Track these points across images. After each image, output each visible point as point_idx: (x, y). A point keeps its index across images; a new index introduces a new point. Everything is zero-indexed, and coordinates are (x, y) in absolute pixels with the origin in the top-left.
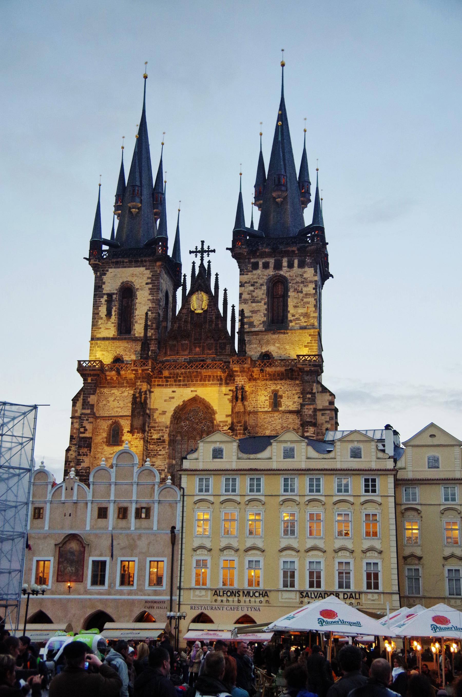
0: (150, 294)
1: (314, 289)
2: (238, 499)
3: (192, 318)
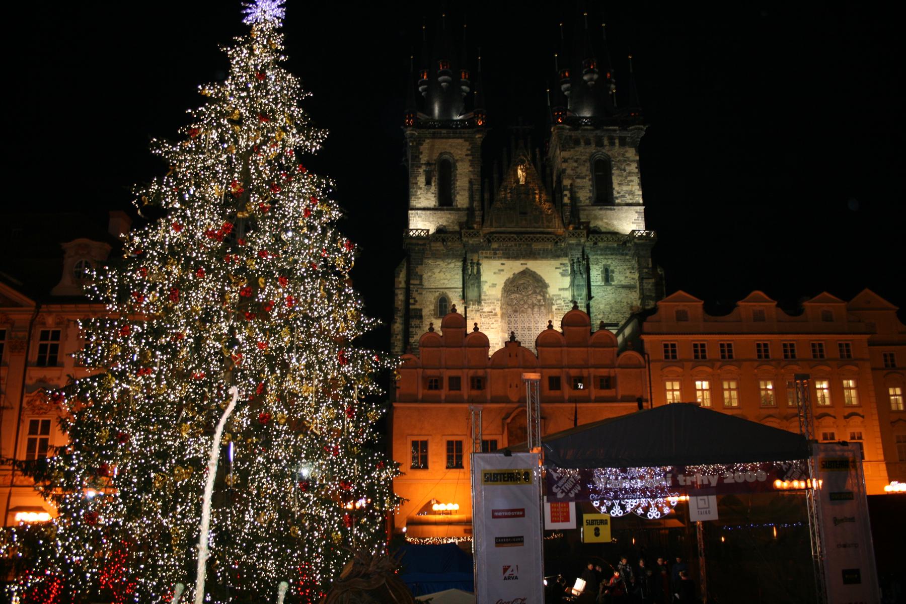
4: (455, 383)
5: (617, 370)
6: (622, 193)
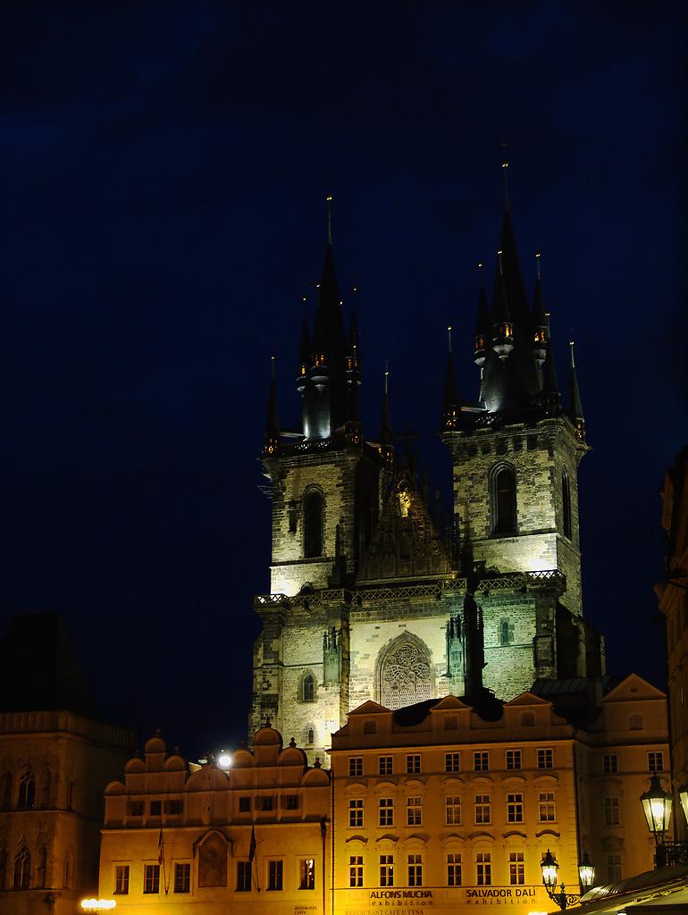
0: (342, 500)
1: (549, 478)
4: (156, 808)
5: (302, 789)
6: (529, 517)
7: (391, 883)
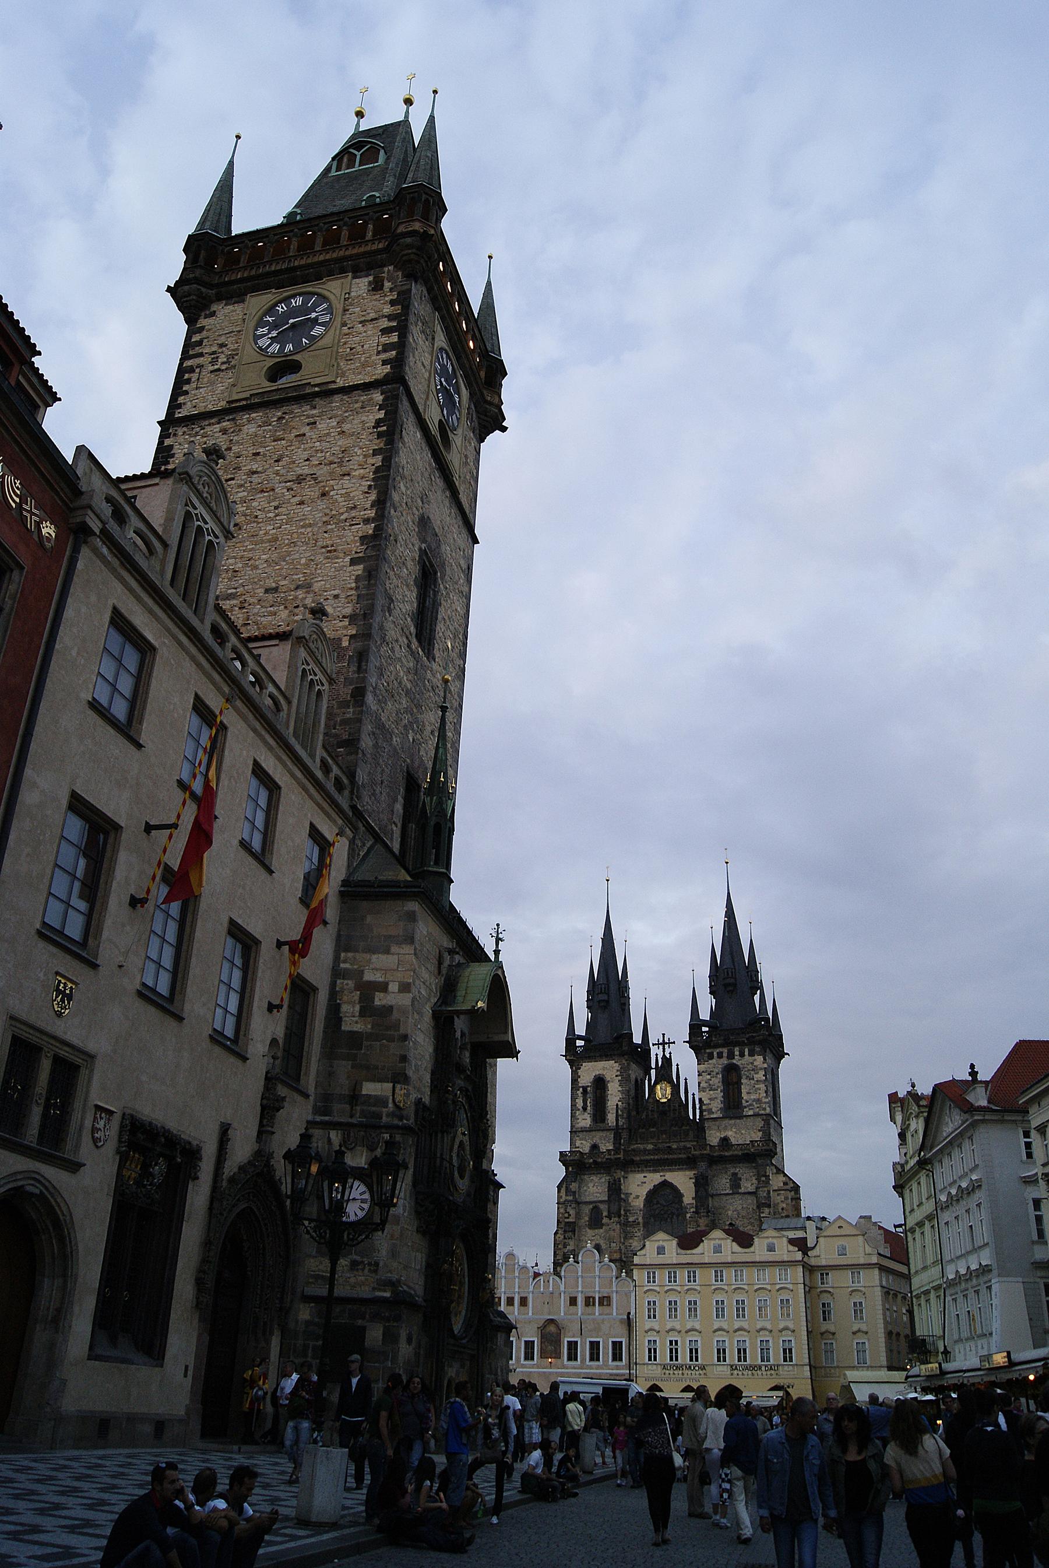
2: (679, 1288)
3: (658, 1107)
7: (677, 1360)
